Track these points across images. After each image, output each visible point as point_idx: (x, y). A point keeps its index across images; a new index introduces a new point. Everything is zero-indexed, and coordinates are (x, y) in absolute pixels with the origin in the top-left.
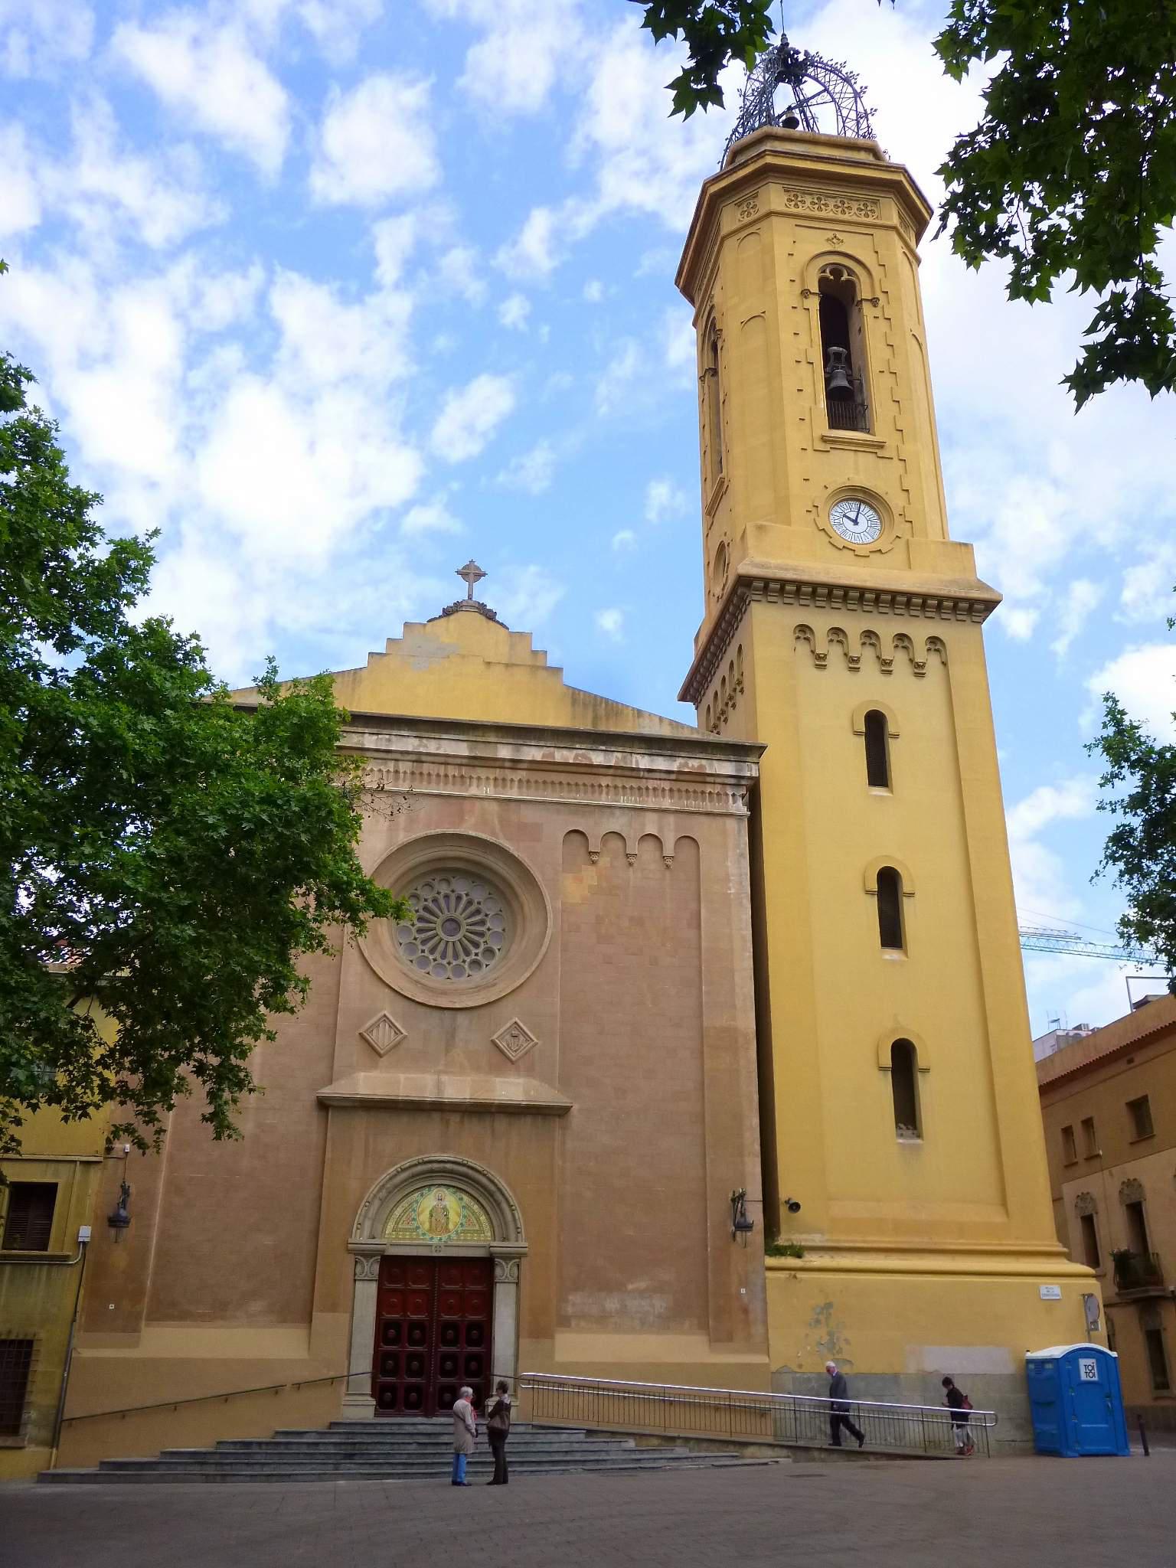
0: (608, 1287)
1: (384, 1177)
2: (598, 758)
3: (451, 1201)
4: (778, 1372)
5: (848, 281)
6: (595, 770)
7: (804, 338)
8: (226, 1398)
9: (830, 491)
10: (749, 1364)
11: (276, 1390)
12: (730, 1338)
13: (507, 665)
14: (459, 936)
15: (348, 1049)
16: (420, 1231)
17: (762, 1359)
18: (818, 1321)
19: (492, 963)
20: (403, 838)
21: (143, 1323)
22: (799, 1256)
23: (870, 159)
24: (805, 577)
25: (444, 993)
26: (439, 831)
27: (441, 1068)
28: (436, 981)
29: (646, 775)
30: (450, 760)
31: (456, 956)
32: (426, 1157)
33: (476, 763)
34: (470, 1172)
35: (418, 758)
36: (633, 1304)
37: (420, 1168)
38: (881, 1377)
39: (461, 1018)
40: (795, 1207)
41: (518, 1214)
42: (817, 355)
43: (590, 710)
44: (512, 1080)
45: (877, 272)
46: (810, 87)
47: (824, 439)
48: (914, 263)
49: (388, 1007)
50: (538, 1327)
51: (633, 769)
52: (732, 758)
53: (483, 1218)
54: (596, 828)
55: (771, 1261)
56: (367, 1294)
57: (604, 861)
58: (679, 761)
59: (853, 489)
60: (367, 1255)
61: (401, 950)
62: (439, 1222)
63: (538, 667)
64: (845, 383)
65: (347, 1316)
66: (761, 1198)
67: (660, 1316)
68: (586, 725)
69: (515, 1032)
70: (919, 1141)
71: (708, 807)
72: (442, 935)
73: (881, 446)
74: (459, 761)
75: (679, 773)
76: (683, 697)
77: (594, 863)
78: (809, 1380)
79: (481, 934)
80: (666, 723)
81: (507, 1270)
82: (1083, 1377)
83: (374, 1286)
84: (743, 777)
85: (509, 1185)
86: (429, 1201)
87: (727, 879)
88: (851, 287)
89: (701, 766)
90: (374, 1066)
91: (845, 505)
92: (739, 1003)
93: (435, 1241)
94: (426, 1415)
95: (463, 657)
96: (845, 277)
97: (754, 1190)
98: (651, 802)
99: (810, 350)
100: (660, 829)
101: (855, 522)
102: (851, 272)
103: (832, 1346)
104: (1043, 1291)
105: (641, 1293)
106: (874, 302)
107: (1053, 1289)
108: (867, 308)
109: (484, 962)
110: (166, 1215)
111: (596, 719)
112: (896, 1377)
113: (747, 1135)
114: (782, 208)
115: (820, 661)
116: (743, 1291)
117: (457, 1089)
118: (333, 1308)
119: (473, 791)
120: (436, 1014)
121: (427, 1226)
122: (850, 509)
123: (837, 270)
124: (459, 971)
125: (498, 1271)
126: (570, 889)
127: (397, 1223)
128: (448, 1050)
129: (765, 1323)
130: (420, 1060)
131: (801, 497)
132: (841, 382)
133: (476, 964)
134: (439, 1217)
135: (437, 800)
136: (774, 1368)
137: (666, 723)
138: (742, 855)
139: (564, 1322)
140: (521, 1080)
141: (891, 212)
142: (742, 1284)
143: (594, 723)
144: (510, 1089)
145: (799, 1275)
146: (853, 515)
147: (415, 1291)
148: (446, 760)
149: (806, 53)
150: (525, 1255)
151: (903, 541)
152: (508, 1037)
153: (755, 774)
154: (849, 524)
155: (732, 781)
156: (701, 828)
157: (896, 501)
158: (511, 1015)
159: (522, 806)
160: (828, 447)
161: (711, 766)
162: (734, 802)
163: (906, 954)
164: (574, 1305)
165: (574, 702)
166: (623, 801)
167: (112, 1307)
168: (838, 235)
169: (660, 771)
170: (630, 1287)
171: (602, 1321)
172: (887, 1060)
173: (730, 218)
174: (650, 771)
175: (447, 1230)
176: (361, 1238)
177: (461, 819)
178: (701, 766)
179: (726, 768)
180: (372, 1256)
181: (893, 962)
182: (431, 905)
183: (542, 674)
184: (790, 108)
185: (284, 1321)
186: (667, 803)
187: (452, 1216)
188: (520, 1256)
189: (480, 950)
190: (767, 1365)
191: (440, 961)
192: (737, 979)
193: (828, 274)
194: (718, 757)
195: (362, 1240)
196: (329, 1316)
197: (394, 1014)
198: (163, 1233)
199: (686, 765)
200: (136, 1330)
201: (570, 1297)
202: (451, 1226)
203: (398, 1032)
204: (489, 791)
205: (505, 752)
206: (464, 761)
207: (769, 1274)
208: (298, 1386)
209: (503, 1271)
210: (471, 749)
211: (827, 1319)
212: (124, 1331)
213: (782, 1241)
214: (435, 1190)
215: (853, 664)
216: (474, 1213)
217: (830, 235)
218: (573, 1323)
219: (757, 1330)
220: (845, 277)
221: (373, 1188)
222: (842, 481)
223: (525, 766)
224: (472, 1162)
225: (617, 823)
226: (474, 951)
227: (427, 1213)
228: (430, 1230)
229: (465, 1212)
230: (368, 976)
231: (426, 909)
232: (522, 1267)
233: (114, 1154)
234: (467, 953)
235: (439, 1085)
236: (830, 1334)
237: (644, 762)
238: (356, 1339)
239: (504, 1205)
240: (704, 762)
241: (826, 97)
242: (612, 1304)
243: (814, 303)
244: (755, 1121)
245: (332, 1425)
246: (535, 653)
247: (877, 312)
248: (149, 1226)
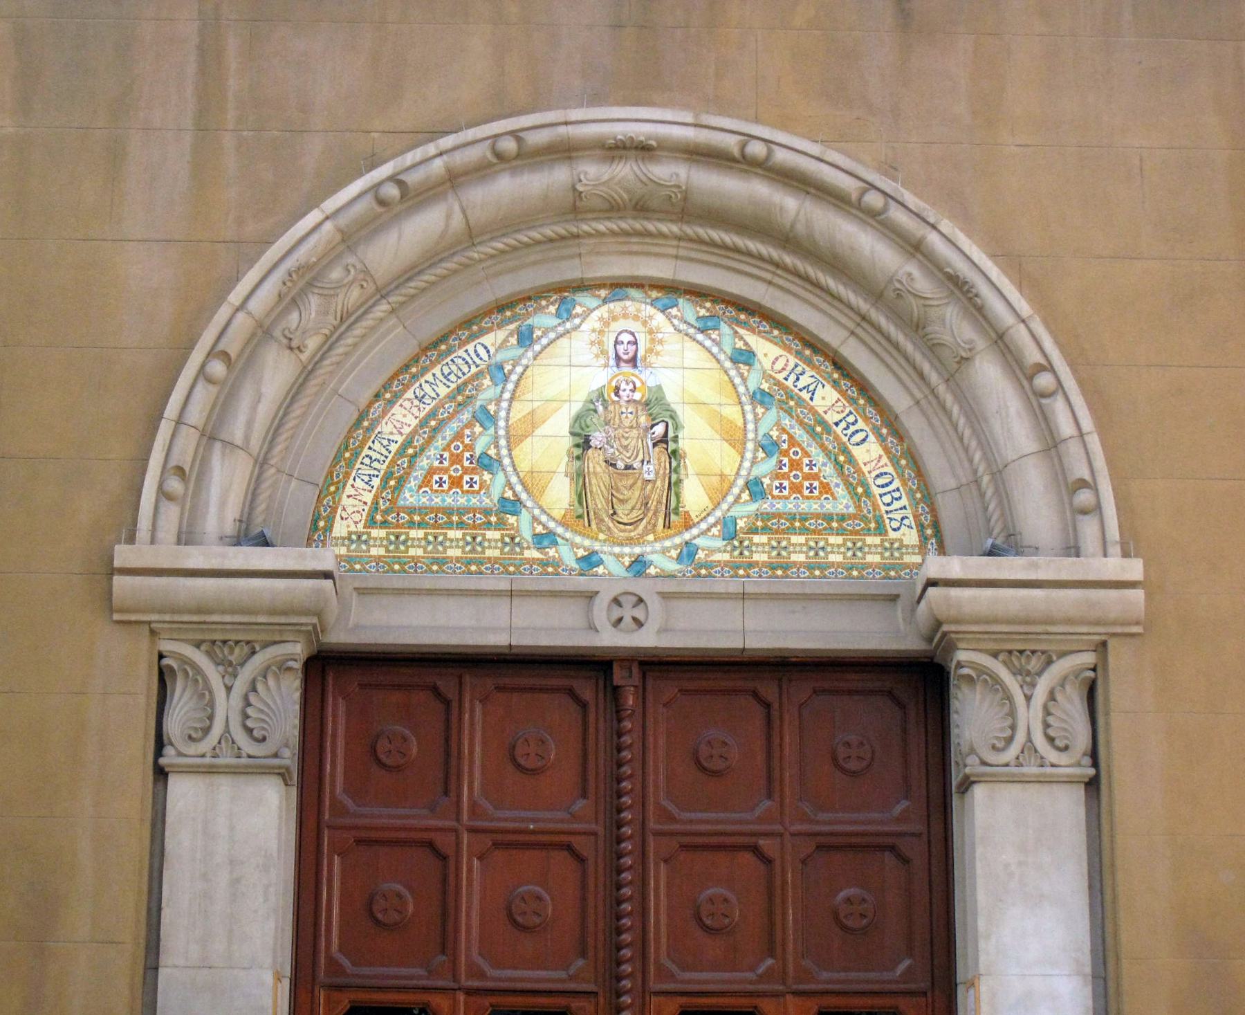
3: (687, 367)
16: (523, 524)
34: (790, 206)
37: (506, 189)
53: (869, 453)
81: (1030, 717)
86: (565, 369)
121: (560, 495)
127: (394, 481)
134: (628, 451)
175: (672, 514)
176: (189, 547)
187: (704, 449)
202: (694, 497)
214: (594, 314)
216: (818, 427)
221: (255, 290)
224: (795, 149)
227: (558, 428)
228: (582, 514)
229: (770, 419)
232: (1120, 695)
239: (988, 373)
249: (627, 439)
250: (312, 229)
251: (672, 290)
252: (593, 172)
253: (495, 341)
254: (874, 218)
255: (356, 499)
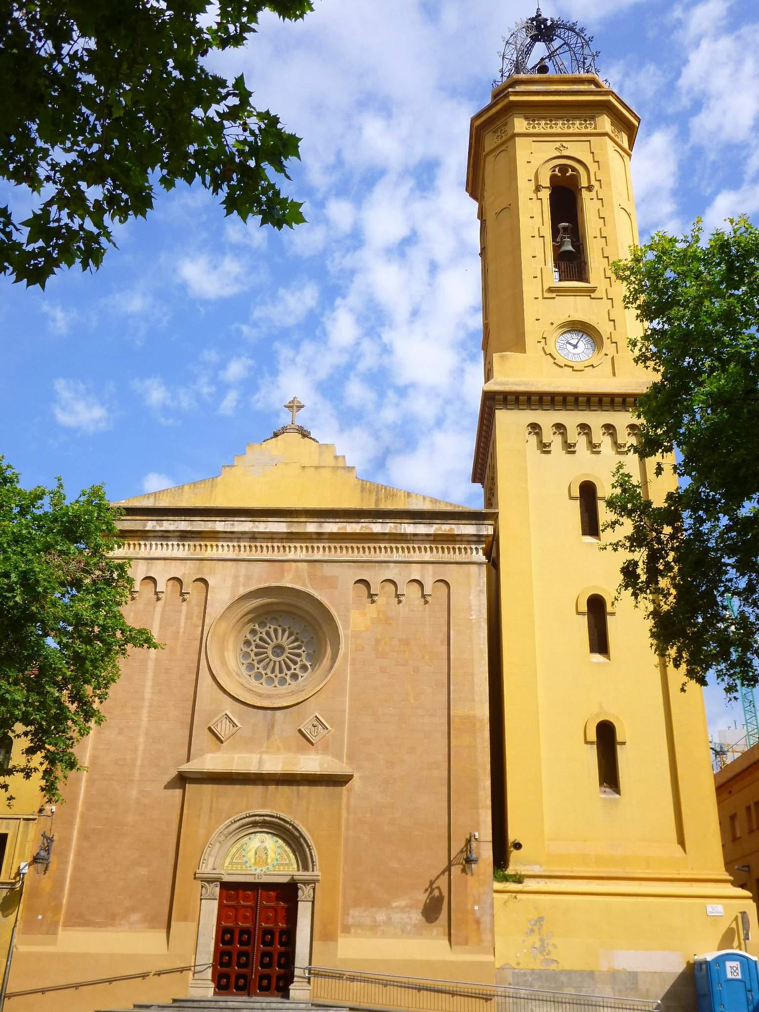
0: (377, 904)
1: (222, 826)
2: (377, 528)
4: (502, 968)
5: (571, 175)
6: (375, 537)
7: (538, 219)
8: (110, 981)
9: (555, 326)
10: (481, 963)
11: (144, 976)
12: (466, 942)
13: (316, 467)
14: (283, 657)
15: (201, 737)
16: (248, 865)
17: (490, 958)
18: (532, 931)
19: (305, 675)
20: (242, 591)
21: (60, 928)
22: (520, 882)
23: (593, 87)
24: (533, 389)
25: (269, 697)
26: (267, 585)
27: (264, 750)
28: (265, 688)
29: (412, 538)
30: (275, 536)
31: (281, 671)
32: (252, 812)
33: (293, 537)
35: (253, 537)
36: (397, 917)
37: (247, 820)
38: (581, 973)
39: (278, 713)
40: (518, 846)
41: (314, 852)
42: (547, 231)
43: (374, 493)
44: (312, 757)
45: (592, 167)
46: (557, 43)
47: (550, 290)
48: (626, 157)
49: (229, 707)
50: (324, 933)
51: (402, 535)
52: (474, 522)
53: (291, 855)
54: (375, 576)
55: (497, 886)
56: (210, 911)
57: (380, 600)
58: (435, 526)
59: (573, 323)
60: (210, 881)
61: (243, 668)
62: (263, 859)
63: (338, 467)
64: (570, 248)
65: (195, 924)
66: (490, 839)
67: (415, 926)
68: (370, 505)
69: (316, 723)
70: (618, 796)
71: (457, 557)
72: (271, 656)
73: (593, 290)
74: (281, 536)
75: (435, 535)
76: (474, 481)
77: (373, 602)
78: (525, 974)
79: (299, 655)
80: (427, 501)
82: (729, 976)
83: (215, 904)
84: (482, 536)
85: (309, 831)
87: (470, 609)
88: (575, 179)
89: (451, 529)
90: (219, 750)
91: (568, 335)
92: (477, 698)
93: (258, 871)
94: (249, 995)
95: (286, 464)
96: (570, 172)
97: (485, 832)
98: (416, 556)
99: (542, 228)
100: (422, 576)
101: (575, 346)
102: (574, 169)
103: (543, 949)
104: (709, 909)
105: (402, 909)
106: (590, 188)
107: (716, 908)
108: (584, 193)
109: (300, 674)
110: (78, 854)
111: (378, 501)
112: (591, 974)
113: (481, 793)
114: (524, 131)
115: (544, 448)
116: (476, 908)
117: (273, 764)
118: (185, 918)
119: (291, 556)
120: (261, 711)
121: (253, 860)
122: (574, 338)
123: (563, 168)
124: (283, 681)
125: (300, 893)
126: (354, 620)
127: (232, 858)
128: (269, 737)
129: (492, 932)
130: (249, 744)
131: (532, 330)
132: (568, 247)
133: (295, 676)
134: (261, 855)
135: (267, 564)
136: (498, 965)
137: (427, 501)
138: (481, 591)
139: (346, 929)
140: (319, 757)
141: (605, 123)
142: (476, 902)
143: (377, 504)
144: (310, 763)
145: (519, 896)
146: (574, 342)
147: (244, 907)
148: (271, 537)
149: (552, 20)
150: (318, 881)
151: (610, 357)
152: (311, 726)
153: (490, 531)
154: (570, 348)
155: (474, 539)
156: (451, 574)
157: (605, 328)
158: (313, 710)
159: (325, 564)
160: (554, 295)
161: (458, 529)
162: (477, 553)
163: (609, 658)
164: (353, 917)
165: (363, 489)
166: (396, 557)
167: (40, 917)
168: (564, 144)
169: (422, 535)
170: (394, 905)
171: (374, 928)
172: (593, 736)
173: (490, 142)
174: (415, 535)
175: (267, 863)
176: (206, 869)
177: (282, 576)
178: (451, 529)
179: (469, 529)
180: (213, 882)
181: (599, 664)
182: (265, 636)
183: (340, 472)
184: (542, 59)
185: (154, 928)
186: (427, 557)
187: (271, 854)
188: (314, 882)
189: (298, 666)
190: (493, 963)
191: (270, 674)
192: (476, 680)
193: (557, 172)
194: (463, 522)
195: (206, 871)
196: (182, 924)
197: (232, 713)
198: (76, 868)
199: (440, 529)
200: (55, 933)
201: (351, 912)
202: (269, 861)
203: (235, 725)
204: (302, 555)
205: (312, 528)
206: (284, 536)
207: (496, 895)
208: (159, 974)
209: (304, 893)
210: (288, 527)
211: (539, 929)
212: (47, 934)
213: (510, 871)
214: (259, 835)
215: (569, 448)
216: (285, 851)
217: (558, 145)
218: (353, 931)
219: (487, 937)
220: (570, 172)
221: (215, 835)
222: (564, 318)
223: (326, 537)
225: (391, 572)
226: (293, 667)
227: (253, 851)
228: (255, 863)
230: (215, 687)
231: (261, 639)
232: (316, 889)
233: (44, 813)
234: (289, 669)
235: (260, 761)
236: (542, 940)
237: (409, 528)
238: (201, 941)
240: (453, 526)
241: (566, 48)
242: (381, 917)
243: (545, 194)
244: (487, 783)
245: (175, 1001)
246: (336, 457)
247: (593, 194)
248: (67, 863)
249: (261, 853)
250: (222, 826)
251: (268, 833)
252: (257, 818)
253: (246, 838)
254: (291, 824)
255: (228, 860)
